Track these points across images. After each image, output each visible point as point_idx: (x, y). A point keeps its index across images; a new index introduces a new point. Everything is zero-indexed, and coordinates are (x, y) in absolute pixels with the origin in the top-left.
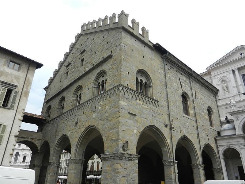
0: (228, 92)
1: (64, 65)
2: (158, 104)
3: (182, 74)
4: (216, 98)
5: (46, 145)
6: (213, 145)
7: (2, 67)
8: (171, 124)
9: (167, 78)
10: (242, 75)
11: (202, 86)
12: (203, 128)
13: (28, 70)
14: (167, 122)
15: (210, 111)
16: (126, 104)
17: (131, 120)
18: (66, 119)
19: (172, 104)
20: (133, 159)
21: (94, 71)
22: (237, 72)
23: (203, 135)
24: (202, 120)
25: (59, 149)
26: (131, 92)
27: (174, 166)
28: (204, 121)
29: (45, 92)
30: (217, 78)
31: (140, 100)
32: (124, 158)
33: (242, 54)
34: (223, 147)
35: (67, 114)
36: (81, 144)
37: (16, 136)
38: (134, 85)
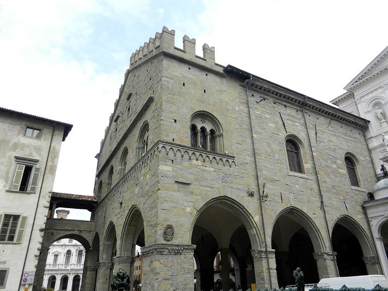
0: (386, 123)
2: (233, 161)
3: (285, 107)
4: (365, 136)
6: (359, 218)
7: (17, 137)
8: (261, 191)
9: (253, 117)
12: (334, 191)
13: (52, 136)
14: (253, 188)
15: (350, 160)
16: (170, 169)
19: (263, 158)
20: (184, 252)
23: (335, 203)
24: (332, 176)
25: (110, 243)
26: (180, 149)
27: (267, 258)
28: (338, 179)
29: (96, 160)
30: (365, 102)
31: (197, 160)
32: (166, 252)
36: (127, 234)
37: (41, 230)
38: (186, 137)
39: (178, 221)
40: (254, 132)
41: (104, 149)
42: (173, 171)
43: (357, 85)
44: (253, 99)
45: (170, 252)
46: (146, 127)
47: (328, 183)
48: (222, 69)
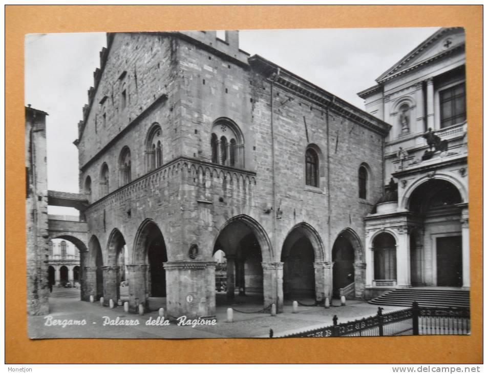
11: (355, 123)
21: (143, 123)
30: (393, 101)
31: (218, 177)
46: (155, 129)
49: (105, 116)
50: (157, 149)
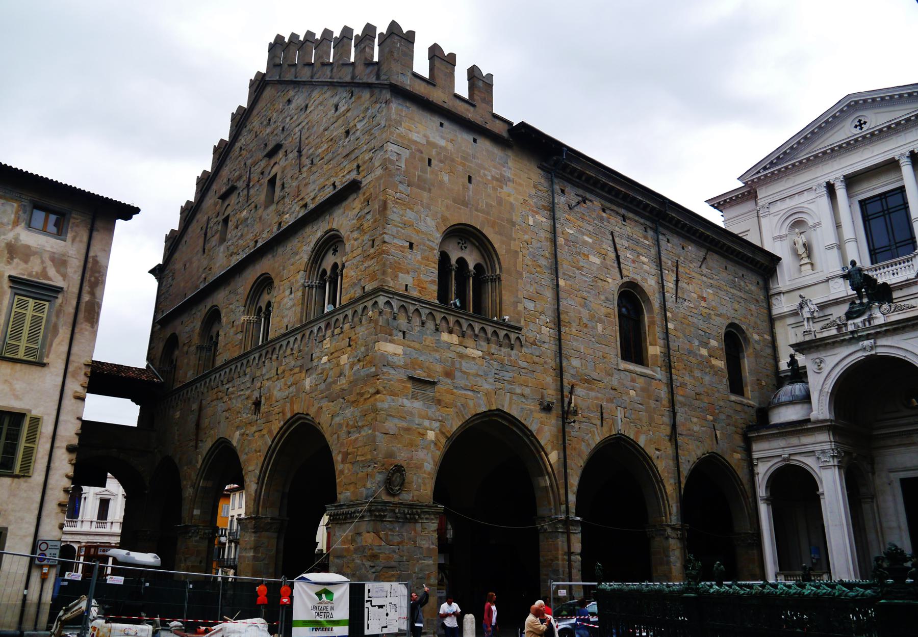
0: (809, 266)
1: (214, 187)
2: (518, 338)
3: (624, 218)
4: (767, 289)
5: (170, 472)
6: (735, 458)
7: (11, 230)
8: (567, 400)
9: (561, 240)
10: (860, 202)
11: (709, 249)
12: (697, 403)
15: (734, 340)
16: (399, 350)
17: (417, 399)
18: (227, 386)
21: (308, 230)
22: (841, 193)
23: (696, 428)
24: (697, 373)
27: (568, 534)
29: (153, 284)
30: (775, 214)
31: (451, 332)
33: (861, 125)
34: (770, 464)
35: (228, 370)
37: (70, 449)
38: (432, 282)
39: (411, 458)
40: (560, 274)
41: (177, 255)
42: (405, 354)
43: (766, 176)
44: (563, 199)
45: (397, 517)
46: (332, 241)
47: (689, 387)
48: (506, 127)
49: (226, 221)
50: (330, 277)
